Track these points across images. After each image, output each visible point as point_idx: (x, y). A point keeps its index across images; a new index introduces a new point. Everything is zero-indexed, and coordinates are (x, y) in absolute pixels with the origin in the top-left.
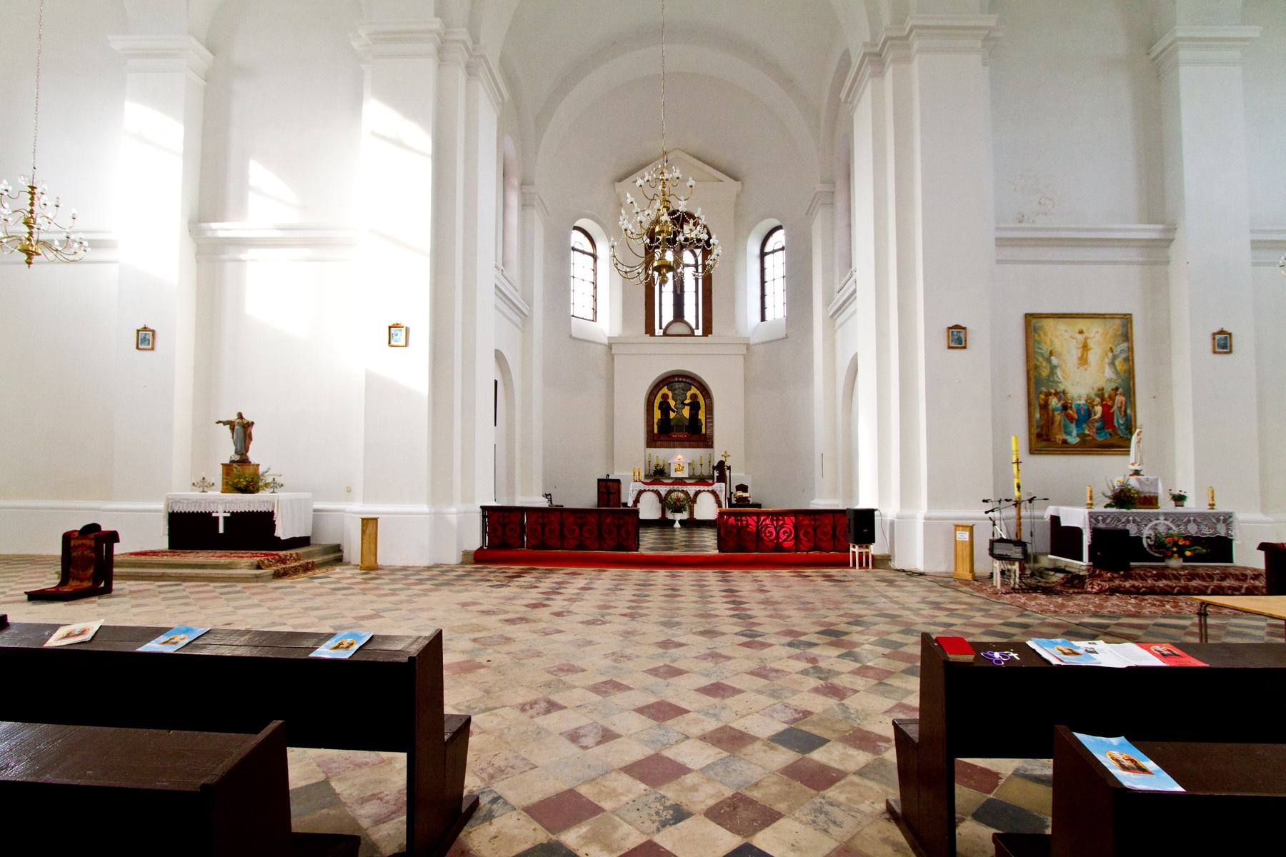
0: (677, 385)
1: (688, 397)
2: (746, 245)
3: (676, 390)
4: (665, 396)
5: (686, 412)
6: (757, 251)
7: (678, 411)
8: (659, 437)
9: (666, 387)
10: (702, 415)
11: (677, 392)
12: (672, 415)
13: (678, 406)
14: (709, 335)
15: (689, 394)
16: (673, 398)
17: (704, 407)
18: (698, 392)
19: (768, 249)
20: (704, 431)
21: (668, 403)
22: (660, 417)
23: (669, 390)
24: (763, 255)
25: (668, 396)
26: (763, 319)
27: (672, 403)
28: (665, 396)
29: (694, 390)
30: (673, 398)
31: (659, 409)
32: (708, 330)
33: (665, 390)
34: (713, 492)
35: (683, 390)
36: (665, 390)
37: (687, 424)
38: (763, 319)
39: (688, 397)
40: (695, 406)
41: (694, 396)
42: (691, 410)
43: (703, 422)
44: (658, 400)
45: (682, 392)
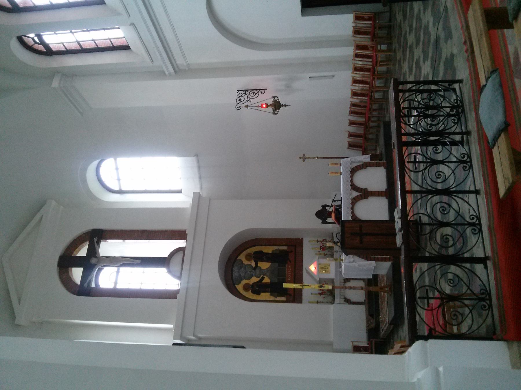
0: (235, 274)
1: (249, 263)
2: (105, 201)
3: (240, 275)
4: (246, 288)
5: (265, 265)
6: (117, 196)
7: (263, 273)
8: (290, 295)
9: (236, 286)
10: (269, 250)
11: (242, 275)
12: (267, 280)
13: (258, 274)
14: (187, 232)
15: (246, 262)
16: (248, 279)
17: (260, 247)
18: (245, 253)
19: (117, 188)
20: (285, 248)
21: (253, 284)
22: (269, 294)
23: (239, 283)
24: (120, 192)
25: (246, 284)
26: (180, 192)
27: (254, 280)
28: (246, 288)
29: (242, 257)
30: (249, 278)
31: (259, 294)
32: (180, 235)
33: (240, 287)
34: (354, 171)
35: (241, 268)
36: (240, 287)
37: (277, 264)
38: (180, 192)
39: (249, 263)
40: (259, 257)
41: (248, 257)
42: (263, 261)
43: (276, 248)
44: (249, 294)
45: (243, 269)
